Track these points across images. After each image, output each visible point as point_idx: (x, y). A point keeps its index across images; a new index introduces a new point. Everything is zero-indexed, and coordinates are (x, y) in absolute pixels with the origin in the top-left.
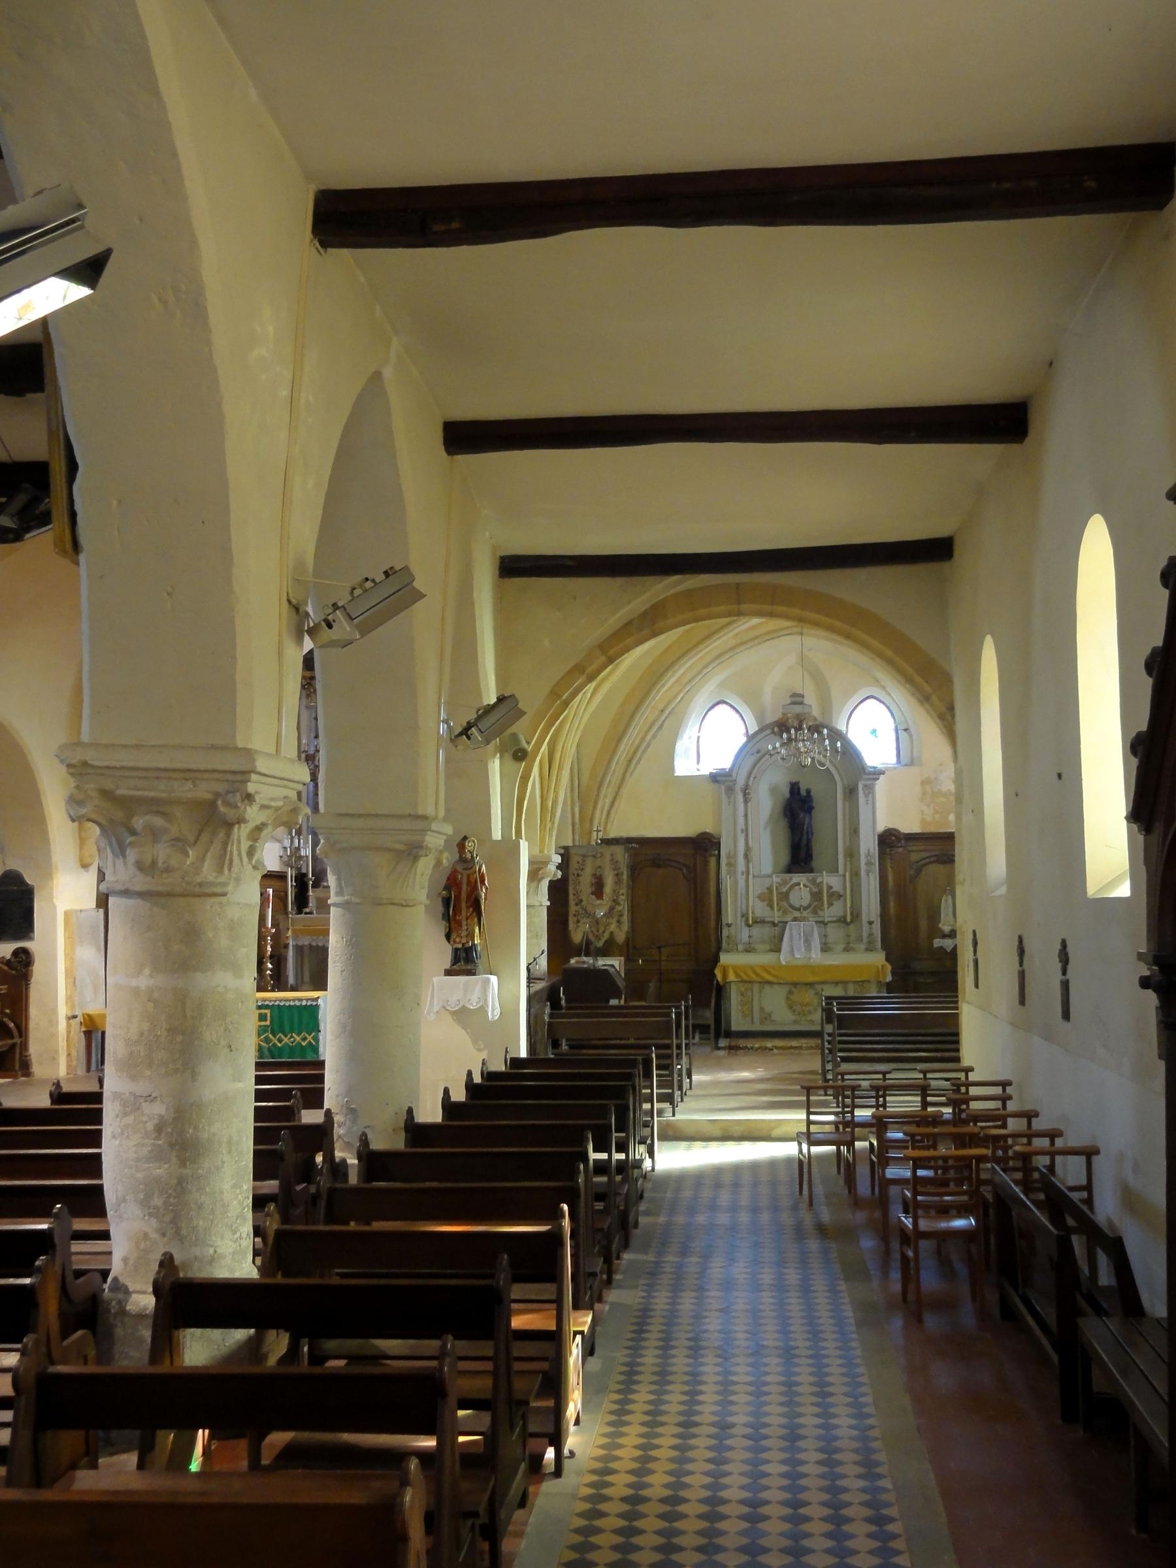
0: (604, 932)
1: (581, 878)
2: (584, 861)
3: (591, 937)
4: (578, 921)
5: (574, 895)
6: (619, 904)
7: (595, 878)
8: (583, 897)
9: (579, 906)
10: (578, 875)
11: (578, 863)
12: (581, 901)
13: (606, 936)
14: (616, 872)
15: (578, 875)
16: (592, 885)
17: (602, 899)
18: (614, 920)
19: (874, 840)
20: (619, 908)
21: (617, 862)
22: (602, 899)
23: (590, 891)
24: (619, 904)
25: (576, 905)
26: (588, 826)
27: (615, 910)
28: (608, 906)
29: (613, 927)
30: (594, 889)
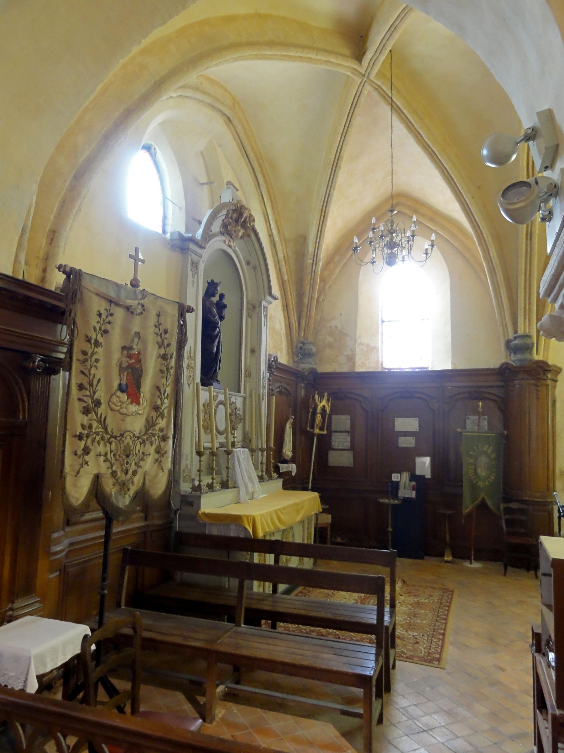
0: (135, 473)
1: (100, 350)
2: (111, 315)
3: (109, 486)
4: (86, 451)
5: (81, 387)
6: (162, 415)
7: (130, 357)
8: (101, 394)
9: (93, 415)
10: (97, 344)
11: (100, 315)
12: (98, 403)
13: (137, 480)
14: (162, 352)
15: (97, 344)
16: (121, 369)
17: (138, 404)
18: (151, 450)
19: (266, 364)
20: (162, 423)
21: (166, 332)
22: (138, 404)
23: (116, 384)
24: (162, 415)
25: (86, 411)
26: (43, 241)
27: (157, 428)
28: (145, 416)
29: (148, 464)
30: (124, 382)
